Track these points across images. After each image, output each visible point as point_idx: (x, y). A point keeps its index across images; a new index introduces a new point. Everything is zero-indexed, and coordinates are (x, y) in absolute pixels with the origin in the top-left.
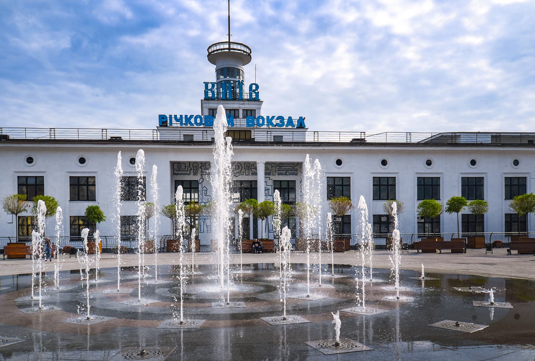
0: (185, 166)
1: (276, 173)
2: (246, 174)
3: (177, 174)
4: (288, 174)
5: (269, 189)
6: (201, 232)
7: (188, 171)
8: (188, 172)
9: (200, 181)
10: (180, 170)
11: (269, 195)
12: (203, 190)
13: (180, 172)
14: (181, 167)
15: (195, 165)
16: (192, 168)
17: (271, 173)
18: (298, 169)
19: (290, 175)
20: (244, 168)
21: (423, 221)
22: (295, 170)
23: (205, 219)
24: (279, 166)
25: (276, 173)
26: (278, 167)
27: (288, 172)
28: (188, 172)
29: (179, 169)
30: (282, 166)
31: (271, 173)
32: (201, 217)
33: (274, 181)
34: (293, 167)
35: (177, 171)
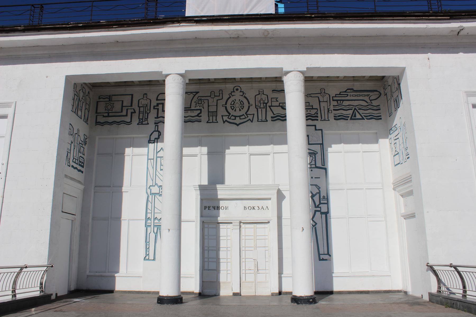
0: (122, 106)
1: (331, 116)
2: (260, 118)
3: (102, 124)
4: (358, 116)
6: (148, 259)
7: (126, 115)
8: (128, 119)
10: (110, 114)
11: (317, 167)
12: (157, 157)
13: (110, 120)
14: (113, 107)
17: (319, 115)
18: (381, 107)
19: (363, 119)
20: (254, 105)
22: (375, 108)
24: (337, 101)
25: (331, 116)
26: (335, 103)
27: (357, 114)
28: (128, 119)
29: (108, 113)
30: (343, 100)
31: (319, 115)
32: (149, 221)
34: (369, 101)
35: (104, 116)
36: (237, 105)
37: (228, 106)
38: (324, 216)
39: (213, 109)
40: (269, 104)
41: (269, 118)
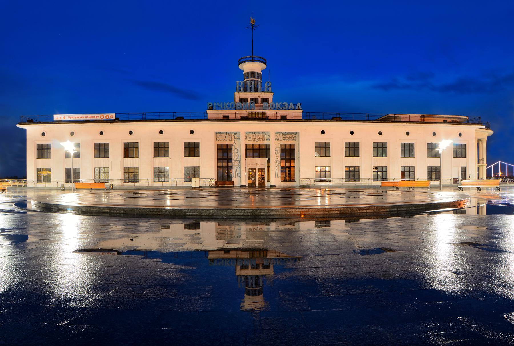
3: (219, 140)
4: (290, 140)
5: (278, 150)
9: (233, 145)
13: (221, 139)
15: (230, 134)
16: (228, 136)
21: (376, 170)
22: (295, 137)
23: (236, 169)
25: (283, 139)
26: (284, 135)
33: (281, 144)
36: (257, 136)
37: (254, 136)
38: (279, 167)
39: (250, 137)
40: (266, 136)
41: (265, 140)
